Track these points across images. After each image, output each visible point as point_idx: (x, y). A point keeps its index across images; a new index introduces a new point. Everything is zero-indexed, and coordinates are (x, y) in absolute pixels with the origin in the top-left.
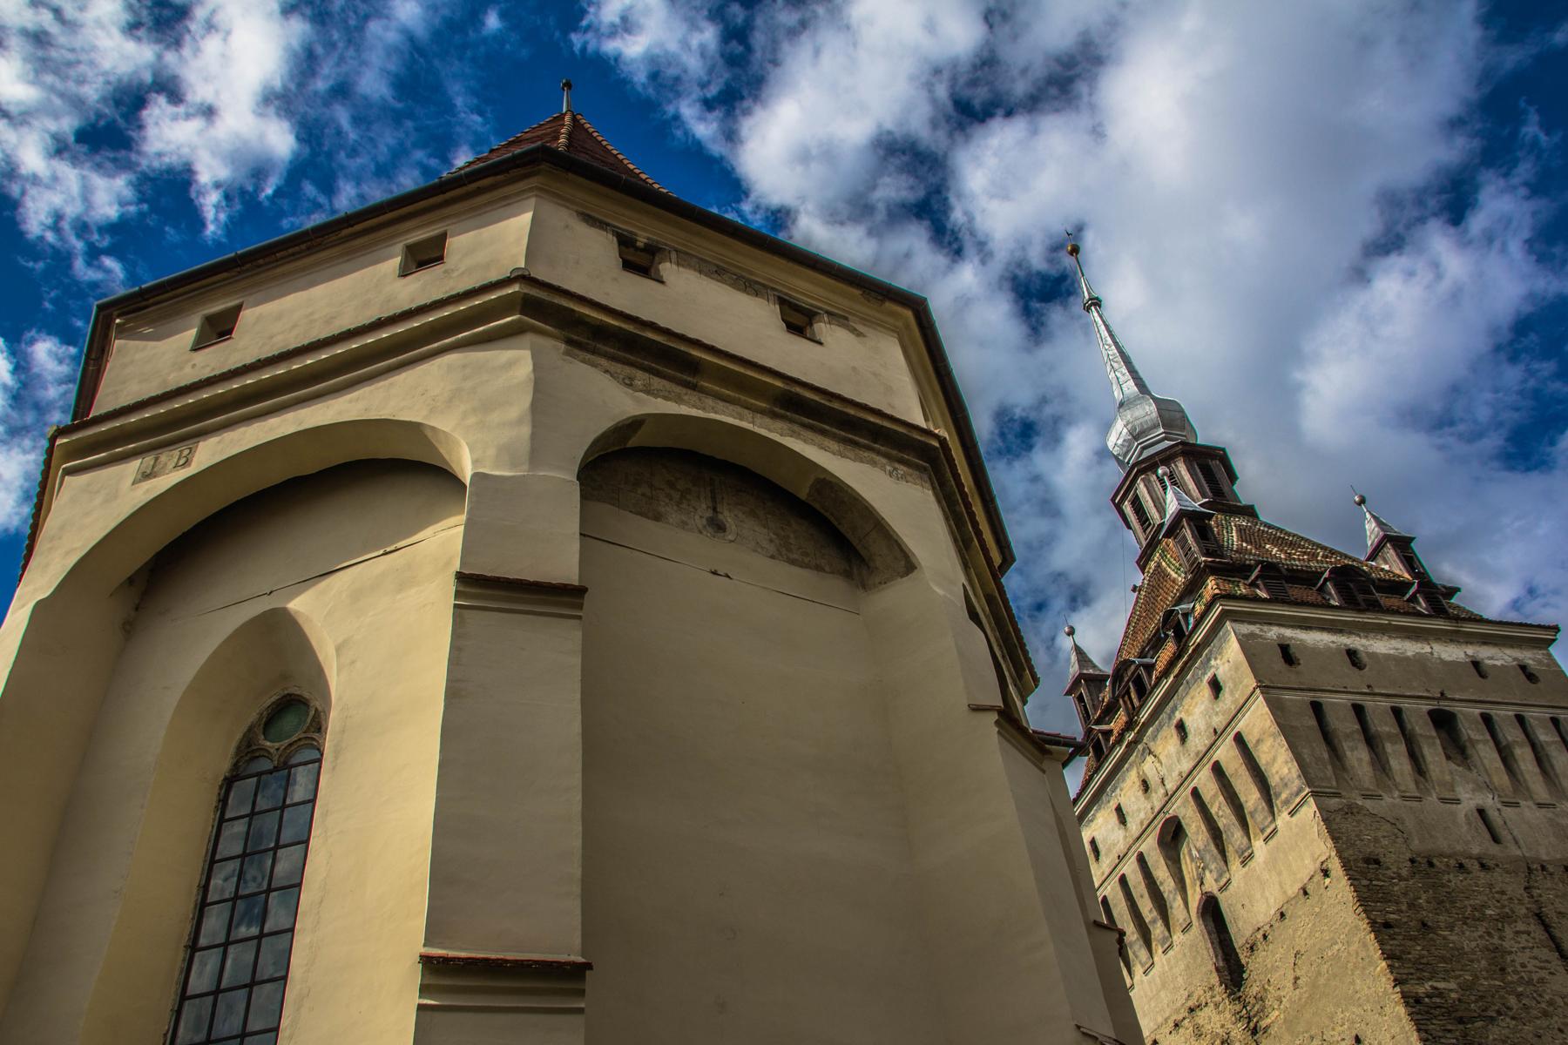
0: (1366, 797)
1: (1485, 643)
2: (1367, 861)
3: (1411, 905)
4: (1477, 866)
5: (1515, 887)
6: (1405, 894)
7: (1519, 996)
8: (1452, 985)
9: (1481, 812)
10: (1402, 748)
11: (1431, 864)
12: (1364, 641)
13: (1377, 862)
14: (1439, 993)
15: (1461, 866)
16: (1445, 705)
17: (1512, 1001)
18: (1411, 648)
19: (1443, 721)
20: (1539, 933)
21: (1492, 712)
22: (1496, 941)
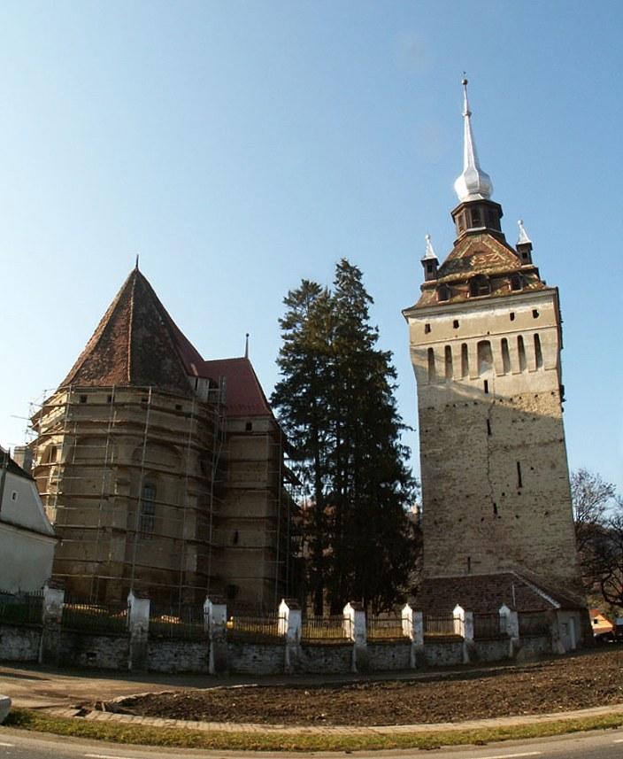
0: (439, 384)
1: (522, 302)
2: (429, 408)
3: (439, 423)
4: (473, 403)
5: (484, 411)
6: (438, 418)
7: (463, 450)
8: (441, 449)
9: (486, 382)
10: (460, 360)
11: (454, 406)
12: (464, 315)
13: (433, 408)
14: (434, 453)
15: (466, 405)
16: (486, 339)
17: (460, 452)
18: (483, 314)
19: (484, 345)
20: (486, 427)
21: (507, 337)
22: (465, 432)
